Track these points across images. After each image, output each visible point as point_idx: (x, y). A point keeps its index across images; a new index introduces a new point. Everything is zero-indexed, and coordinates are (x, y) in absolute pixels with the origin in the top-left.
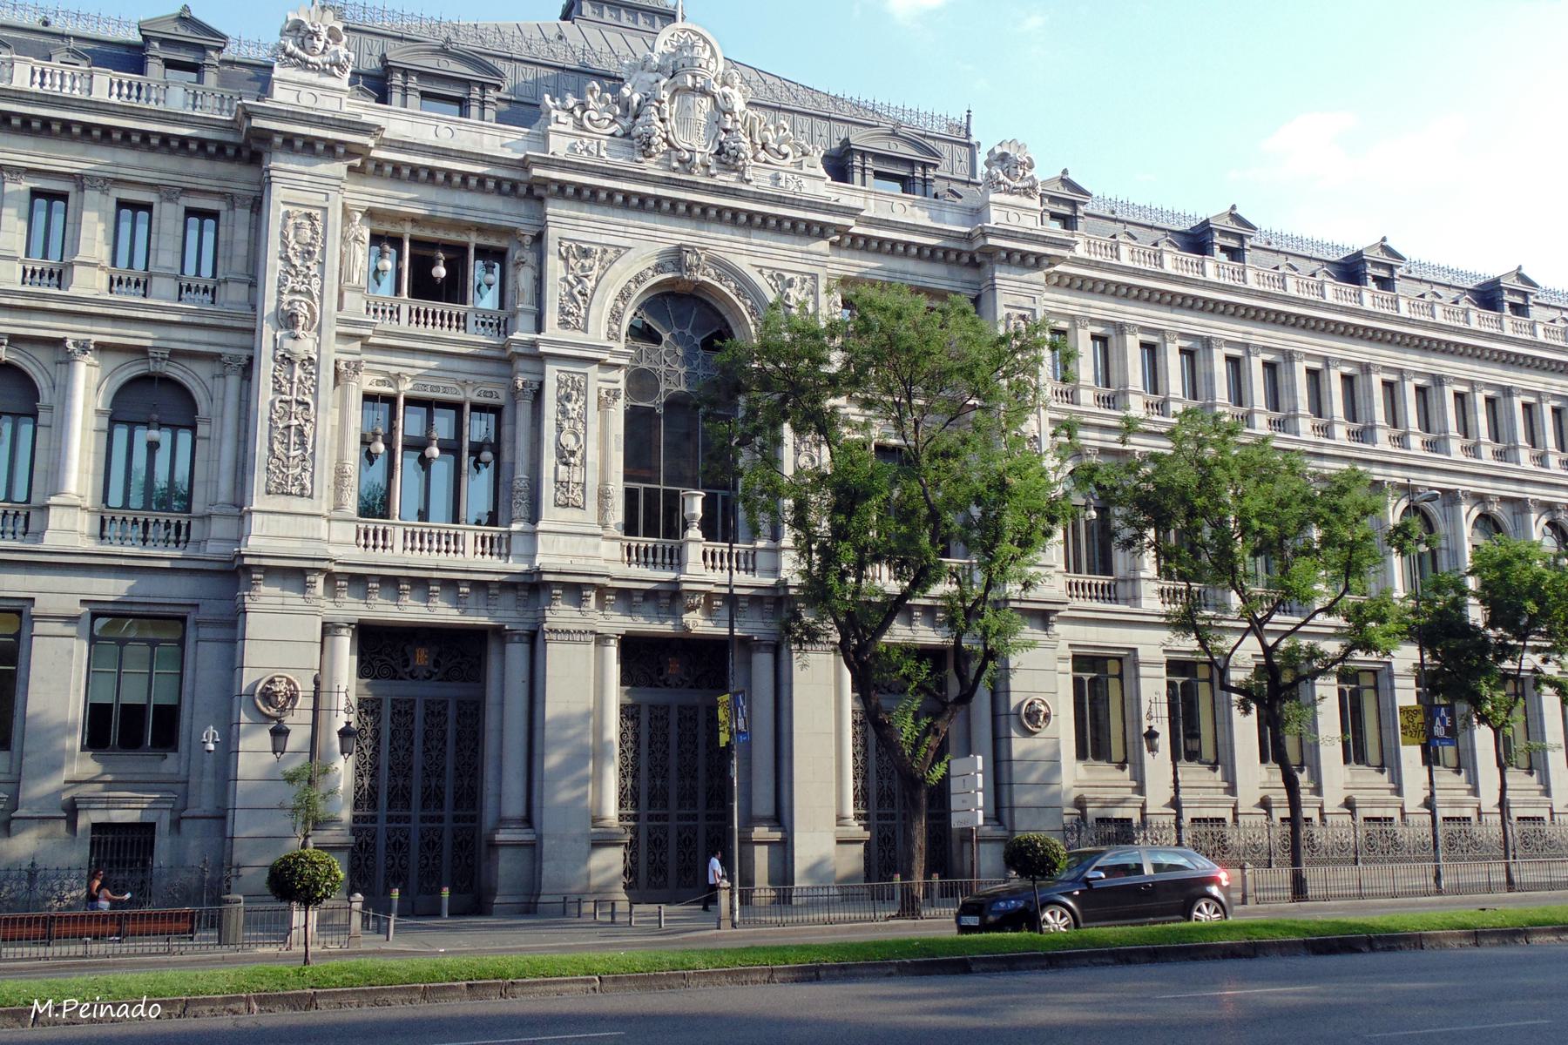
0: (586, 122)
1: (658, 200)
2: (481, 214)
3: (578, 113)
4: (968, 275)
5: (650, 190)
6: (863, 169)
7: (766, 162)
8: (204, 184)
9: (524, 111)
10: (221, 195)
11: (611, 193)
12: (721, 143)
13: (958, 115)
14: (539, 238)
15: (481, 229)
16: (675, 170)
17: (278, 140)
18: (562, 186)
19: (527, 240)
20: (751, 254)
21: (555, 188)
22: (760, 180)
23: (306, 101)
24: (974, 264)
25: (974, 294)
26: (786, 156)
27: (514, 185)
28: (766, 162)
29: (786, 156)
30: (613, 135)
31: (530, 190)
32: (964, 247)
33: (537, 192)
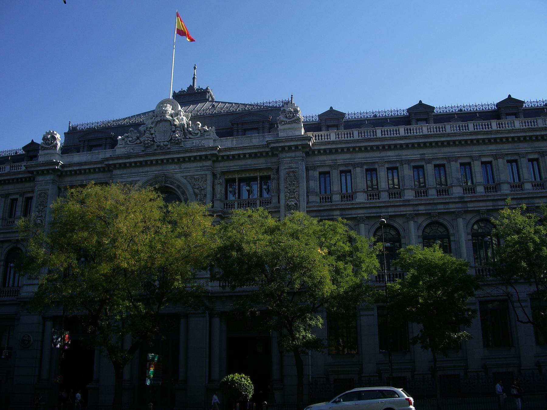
0: (128, 142)
1: (146, 162)
3: (126, 140)
4: (274, 160)
5: (141, 159)
6: (237, 130)
7: (190, 138)
11: (130, 163)
13: (287, 98)
16: (156, 150)
18: (115, 165)
20: (181, 172)
21: (113, 166)
22: (188, 144)
24: (274, 155)
25: (276, 167)
27: (104, 168)
28: (190, 138)
32: (267, 150)
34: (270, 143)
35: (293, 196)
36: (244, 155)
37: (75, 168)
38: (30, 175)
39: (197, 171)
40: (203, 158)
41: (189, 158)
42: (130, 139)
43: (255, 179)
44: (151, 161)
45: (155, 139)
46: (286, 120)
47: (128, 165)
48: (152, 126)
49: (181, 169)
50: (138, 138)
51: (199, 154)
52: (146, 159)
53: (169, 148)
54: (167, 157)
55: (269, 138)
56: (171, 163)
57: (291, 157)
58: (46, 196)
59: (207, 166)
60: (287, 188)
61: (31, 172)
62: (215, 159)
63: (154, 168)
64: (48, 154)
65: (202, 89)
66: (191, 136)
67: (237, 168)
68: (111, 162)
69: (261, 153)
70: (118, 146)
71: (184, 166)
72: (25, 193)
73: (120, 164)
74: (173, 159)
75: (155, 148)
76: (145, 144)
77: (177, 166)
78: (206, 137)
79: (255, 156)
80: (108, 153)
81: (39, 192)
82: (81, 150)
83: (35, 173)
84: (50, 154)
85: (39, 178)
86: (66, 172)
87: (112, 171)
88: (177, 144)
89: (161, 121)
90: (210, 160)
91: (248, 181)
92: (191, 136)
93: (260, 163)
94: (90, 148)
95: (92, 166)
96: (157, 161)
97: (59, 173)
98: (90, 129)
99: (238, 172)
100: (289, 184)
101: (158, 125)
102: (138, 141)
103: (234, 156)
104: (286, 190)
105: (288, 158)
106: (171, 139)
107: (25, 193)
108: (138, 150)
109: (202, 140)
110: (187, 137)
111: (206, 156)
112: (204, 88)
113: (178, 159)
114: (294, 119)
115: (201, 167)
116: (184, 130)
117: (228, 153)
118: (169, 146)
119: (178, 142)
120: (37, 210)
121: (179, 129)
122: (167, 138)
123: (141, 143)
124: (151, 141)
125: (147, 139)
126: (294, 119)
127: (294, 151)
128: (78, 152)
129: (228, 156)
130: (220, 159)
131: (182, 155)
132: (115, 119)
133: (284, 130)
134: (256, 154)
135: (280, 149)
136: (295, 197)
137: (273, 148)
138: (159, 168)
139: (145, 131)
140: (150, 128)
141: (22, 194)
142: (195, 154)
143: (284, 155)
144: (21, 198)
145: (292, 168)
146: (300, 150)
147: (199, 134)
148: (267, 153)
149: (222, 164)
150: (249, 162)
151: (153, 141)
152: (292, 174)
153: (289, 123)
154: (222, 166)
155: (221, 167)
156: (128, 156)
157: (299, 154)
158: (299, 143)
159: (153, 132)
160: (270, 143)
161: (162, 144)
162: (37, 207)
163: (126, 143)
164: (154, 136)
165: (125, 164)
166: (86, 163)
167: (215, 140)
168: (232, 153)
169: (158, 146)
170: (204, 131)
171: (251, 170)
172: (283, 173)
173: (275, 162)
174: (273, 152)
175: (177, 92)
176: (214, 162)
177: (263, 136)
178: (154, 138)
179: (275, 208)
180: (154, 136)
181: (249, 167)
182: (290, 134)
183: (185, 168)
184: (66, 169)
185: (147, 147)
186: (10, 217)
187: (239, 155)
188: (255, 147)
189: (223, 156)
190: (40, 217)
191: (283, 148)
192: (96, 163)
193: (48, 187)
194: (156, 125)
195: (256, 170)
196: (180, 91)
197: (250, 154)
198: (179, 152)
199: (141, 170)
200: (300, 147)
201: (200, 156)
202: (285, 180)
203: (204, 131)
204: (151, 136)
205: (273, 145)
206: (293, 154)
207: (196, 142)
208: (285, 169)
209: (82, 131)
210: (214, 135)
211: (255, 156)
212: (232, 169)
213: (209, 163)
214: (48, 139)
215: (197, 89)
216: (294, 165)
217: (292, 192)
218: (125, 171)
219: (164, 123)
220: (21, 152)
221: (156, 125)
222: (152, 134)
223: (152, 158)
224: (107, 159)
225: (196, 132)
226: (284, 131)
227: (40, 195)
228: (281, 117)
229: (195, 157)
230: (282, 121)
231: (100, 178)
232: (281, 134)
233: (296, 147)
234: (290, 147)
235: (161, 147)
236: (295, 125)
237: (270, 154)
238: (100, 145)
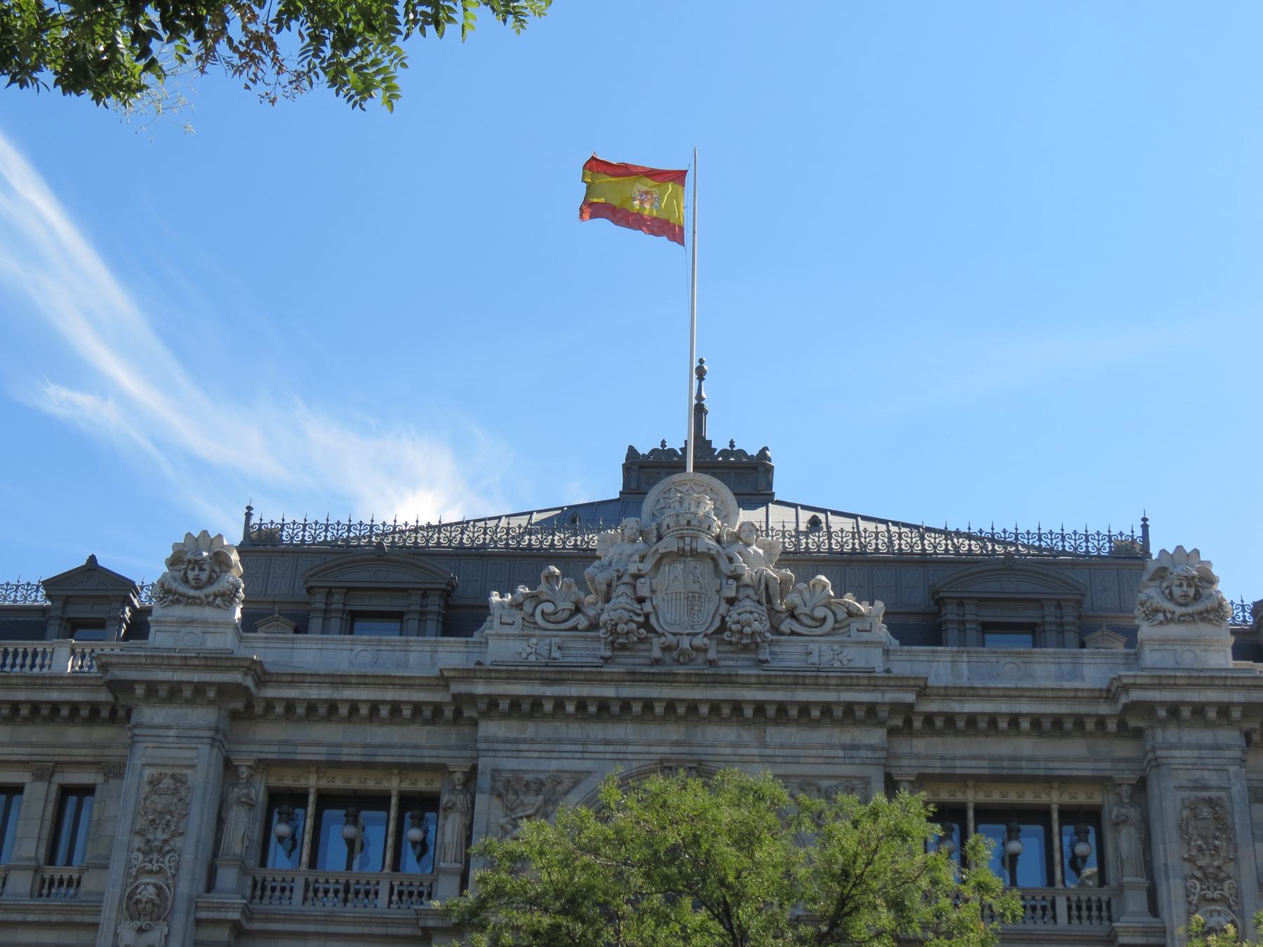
1: (626, 704)
2: (398, 751)
3: (528, 607)
4: (1124, 749)
5: (609, 692)
7: (793, 633)
8: (80, 754)
9: (461, 617)
10: (97, 765)
11: (560, 703)
12: (723, 619)
13: (1127, 526)
14: (472, 774)
15: (402, 768)
16: (657, 662)
17: (140, 691)
18: (493, 701)
19: (458, 777)
20: (768, 760)
23: (188, 640)
25: (1130, 777)
26: (824, 620)
27: (437, 708)
28: (793, 633)
29: (824, 620)
30: (575, 629)
31: (458, 713)
32: (1104, 709)
33: (468, 713)
34: (1126, 688)
35: (1216, 895)
36: (1014, 719)
37: (314, 693)
38: (104, 696)
39: (828, 760)
40: (860, 713)
41: (804, 708)
42: (549, 608)
43: (1039, 815)
44: (648, 704)
45: (653, 620)
46: (1170, 606)
47: (548, 707)
48: (646, 567)
49: (765, 746)
50: (578, 610)
51: (847, 696)
52: (627, 692)
53: (711, 663)
54: (719, 693)
55: (1093, 670)
56: (723, 721)
57: (1200, 747)
58: (183, 793)
59: (873, 748)
60: (1190, 860)
61: (120, 687)
62: (898, 722)
63: (653, 731)
64: (191, 622)
65: (742, 452)
66: (797, 628)
67: (982, 768)
68: (481, 689)
69: (1079, 721)
70: (492, 626)
71: (776, 734)
72: (58, 766)
73: (516, 702)
74: (737, 707)
75: (657, 653)
76: (618, 635)
77: (747, 735)
78: (855, 636)
79: (1055, 727)
80: (452, 653)
81: (148, 772)
82: (316, 623)
83: (140, 691)
84: (204, 622)
85: (151, 714)
86: (270, 704)
87: (474, 723)
88: (746, 648)
89: (681, 554)
90: (881, 724)
91: (1009, 818)
92: (797, 628)
93: (1070, 755)
94: (353, 620)
95: (390, 695)
96: (671, 705)
97: (239, 705)
98: (333, 544)
99: (978, 780)
100: (1200, 849)
101: (665, 569)
102: (581, 621)
103: (972, 719)
104: (1187, 869)
105: (1190, 747)
106: (723, 627)
107: (58, 766)
108: (583, 651)
109: (843, 644)
110: (785, 627)
111: (871, 708)
112: (753, 451)
113: (760, 707)
114: (1200, 607)
115: (844, 747)
116: (769, 600)
117: (956, 707)
118: (712, 655)
119: (750, 645)
120: (138, 842)
121: (750, 592)
122: (706, 619)
123: (594, 626)
124: (640, 626)
125: (626, 615)
126: (1200, 607)
127: (1209, 725)
128: (301, 628)
129: (950, 719)
130: (918, 723)
131: (779, 696)
132: (423, 523)
133: (1164, 641)
134: (1058, 721)
135: (1162, 713)
136: (1223, 899)
137: (1131, 707)
138: (673, 732)
139: (609, 585)
140: (636, 577)
141: (44, 771)
142: (830, 696)
143: (1172, 734)
144: (41, 787)
145: (1205, 788)
146: (1231, 723)
147: (830, 623)
148: (1101, 721)
149: (920, 745)
150: (1026, 746)
151: (646, 625)
152: (1206, 812)
153: (1181, 620)
154: (924, 751)
155: (917, 756)
156: (557, 673)
157: (1230, 736)
158: (1238, 696)
159: (644, 591)
160: (1126, 688)
161: (685, 643)
162: (140, 833)
163: (529, 621)
164: (647, 607)
165: (537, 702)
166: (364, 680)
167: (887, 652)
168: (971, 707)
169: (666, 649)
170: (850, 614)
171: (1032, 780)
172: (1169, 802)
173: (1126, 760)
174: (1131, 719)
175: (644, 450)
176: (892, 732)
177: (1074, 656)
178: (647, 616)
179: (1146, 932)
180: (647, 607)
181: (1026, 769)
182: (1188, 659)
183: (782, 746)
184: (270, 693)
185: (623, 647)
186: (51, 860)
187: (993, 719)
188: (1038, 695)
189: (929, 718)
190: (150, 872)
191: (1174, 710)
192: (407, 683)
193: (188, 754)
194: (658, 565)
195: (1048, 781)
196: (654, 451)
197: (1036, 721)
198: (766, 683)
199: (596, 731)
200: (1236, 714)
201: (849, 708)
202: (1183, 828)
203: (850, 614)
204: (637, 607)
205: (1135, 695)
206: (1207, 737)
207: (823, 651)
208: (1178, 788)
209: (299, 551)
210: (881, 631)
211: (1055, 727)
212: (961, 767)
213: (876, 736)
214: (198, 564)
215: (723, 452)
216: (1210, 777)
217: (1213, 878)
218: (530, 729)
219: (691, 563)
220: (40, 599)
221: (658, 565)
222: (641, 600)
223: (653, 692)
224: (467, 675)
225: (820, 612)
226: (1165, 647)
227: (154, 782)
228: (1152, 594)
229: (827, 709)
230: (1156, 611)
231: (417, 747)
232: (1151, 657)
233: (1224, 710)
234: (1199, 710)
235: (683, 653)
236: (1203, 629)
237: (1112, 726)
238: (398, 616)
